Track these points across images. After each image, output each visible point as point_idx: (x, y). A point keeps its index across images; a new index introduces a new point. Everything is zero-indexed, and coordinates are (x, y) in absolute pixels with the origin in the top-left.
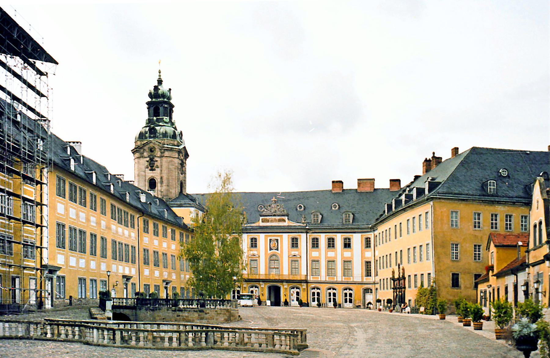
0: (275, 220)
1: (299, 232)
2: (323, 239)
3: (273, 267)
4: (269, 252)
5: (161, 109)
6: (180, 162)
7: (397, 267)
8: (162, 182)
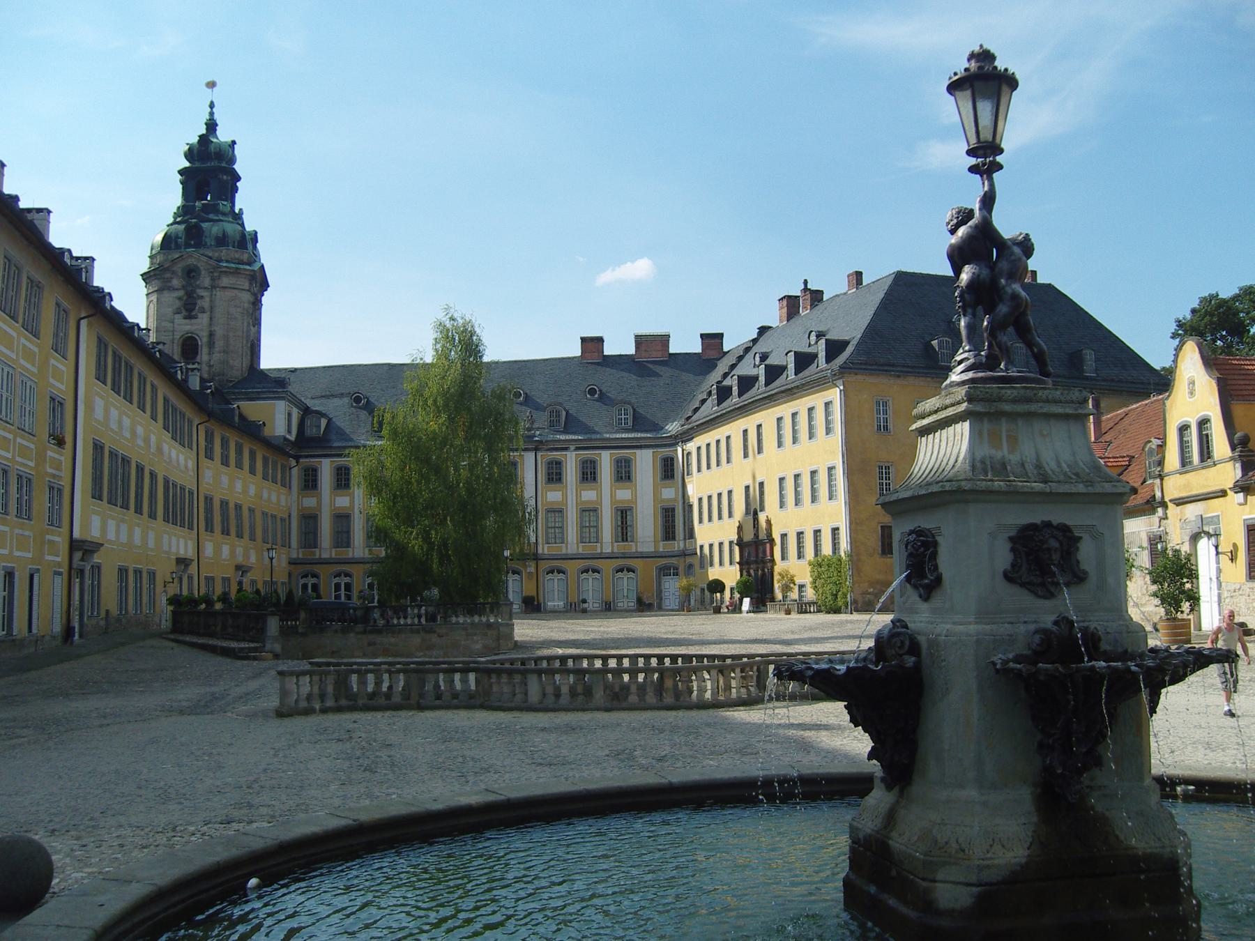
2: (571, 463)
7: (751, 517)
8: (211, 344)
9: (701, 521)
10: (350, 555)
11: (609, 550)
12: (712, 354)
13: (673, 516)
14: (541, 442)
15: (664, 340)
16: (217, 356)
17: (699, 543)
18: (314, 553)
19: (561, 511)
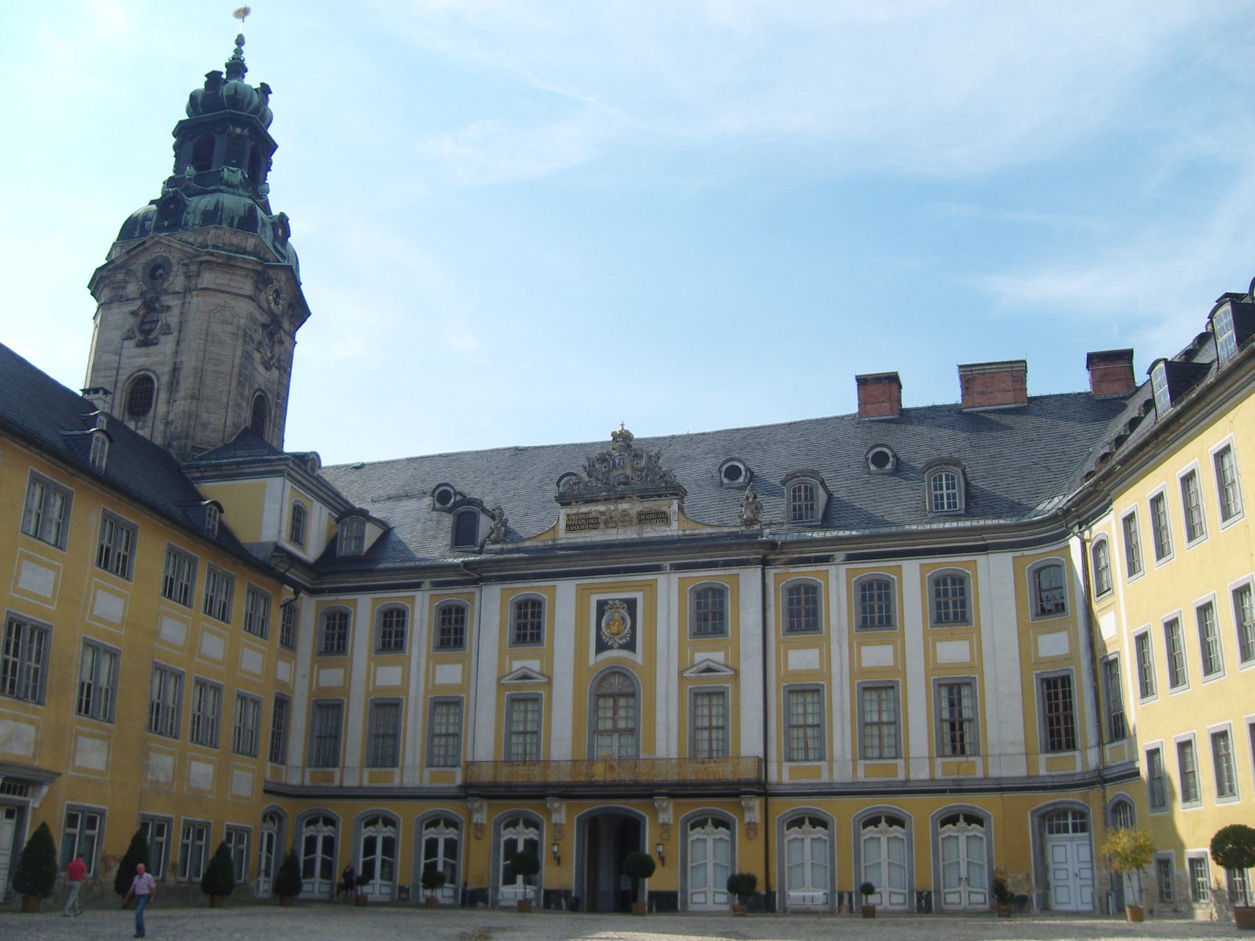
0: (625, 520)
1: (727, 564)
2: (837, 586)
3: (609, 725)
4: (592, 658)
5: (220, 143)
6: (263, 318)
8: (174, 385)
9: (1146, 689)
10: (396, 782)
11: (924, 775)
12: (1113, 390)
13: (1067, 695)
14: (773, 545)
15: (1016, 371)
16: (181, 405)
17: (1143, 744)
18: (330, 778)
19: (816, 691)
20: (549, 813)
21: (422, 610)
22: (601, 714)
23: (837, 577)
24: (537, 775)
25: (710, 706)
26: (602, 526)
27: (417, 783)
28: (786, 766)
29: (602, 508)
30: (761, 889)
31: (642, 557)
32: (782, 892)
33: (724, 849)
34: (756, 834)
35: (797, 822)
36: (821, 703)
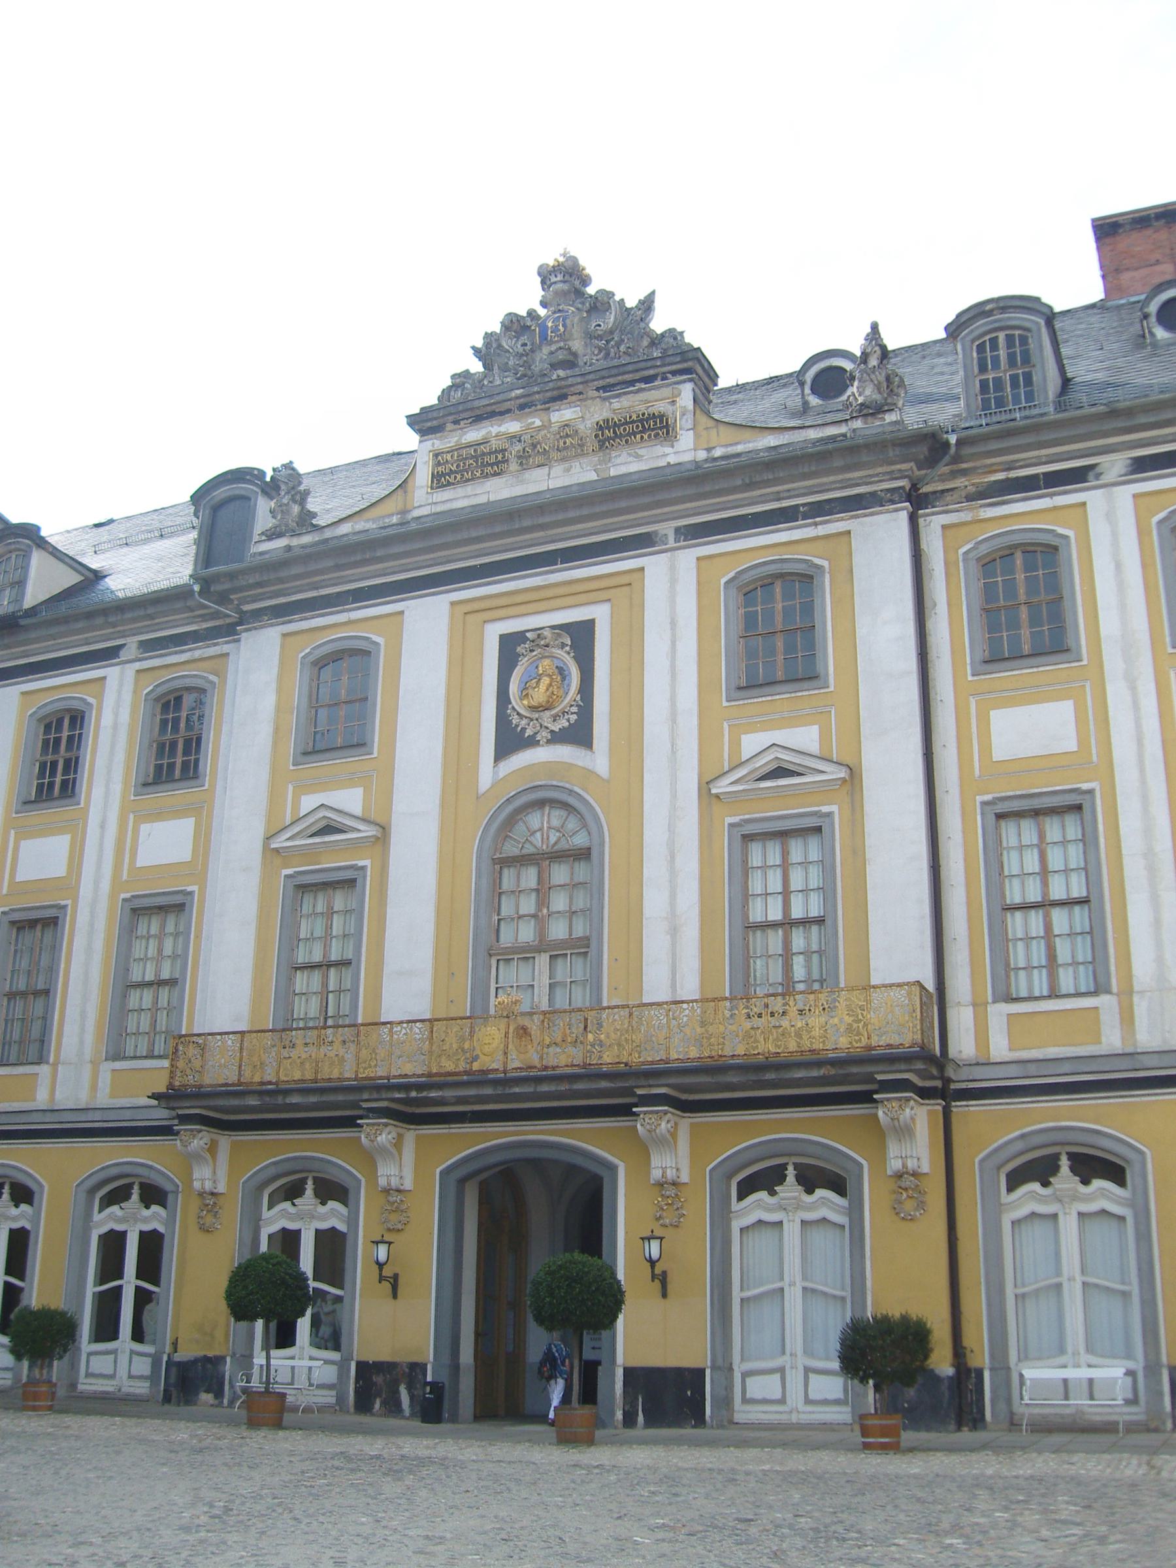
1: (819, 510)
3: (527, 933)
4: (487, 772)
10: (42, 1099)
20: (369, 1160)
21: (117, 704)
22: (507, 909)
23: (1110, 517)
24: (341, 1062)
25: (785, 866)
26: (513, 466)
27: (82, 1098)
28: (999, 1012)
29: (512, 426)
30: (942, 1363)
31: (608, 525)
32: (1002, 1368)
33: (830, 1250)
34: (921, 1205)
35: (1039, 1170)
36: (1088, 841)
